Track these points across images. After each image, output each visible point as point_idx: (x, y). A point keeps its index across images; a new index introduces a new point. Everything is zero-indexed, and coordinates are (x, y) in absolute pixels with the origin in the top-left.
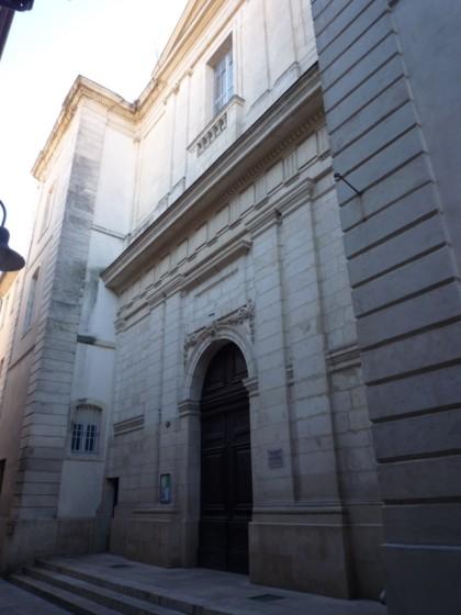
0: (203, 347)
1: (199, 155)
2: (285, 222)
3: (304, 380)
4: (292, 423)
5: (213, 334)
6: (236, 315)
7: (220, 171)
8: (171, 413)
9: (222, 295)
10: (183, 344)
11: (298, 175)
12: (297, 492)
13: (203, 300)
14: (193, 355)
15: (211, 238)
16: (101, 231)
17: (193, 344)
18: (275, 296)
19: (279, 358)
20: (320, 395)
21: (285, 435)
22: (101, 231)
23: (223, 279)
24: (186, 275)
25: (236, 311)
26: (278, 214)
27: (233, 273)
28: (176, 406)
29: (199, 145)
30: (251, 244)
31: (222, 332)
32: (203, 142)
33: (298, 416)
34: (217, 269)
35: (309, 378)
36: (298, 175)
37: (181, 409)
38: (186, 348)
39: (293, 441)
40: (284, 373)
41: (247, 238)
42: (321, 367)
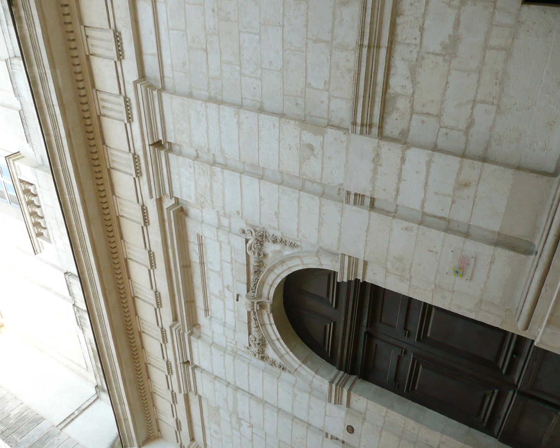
0: (273, 331)
1: (49, 240)
2: (171, 138)
3: (373, 180)
4: (424, 220)
5: (262, 306)
7: (73, 202)
10: (262, 363)
11: (125, 98)
12: (520, 247)
13: (216, 305)
14: (276, 350)
15: (140, 219)
16: (70, 419)
17: (262, 344)
18: (252, 185)
19: (332, 209)
20: (403, 160)
21: (435, 236)
22: (70, 419)
23: (202, 264)
24: (175, 319)
25: (248, 256)
26: (158, 144)
27: (201, 245)
28: (332, 408)
29: (39, 235)
30: (177, 199)
31: (265, 291)
32: (38, 227)
33: (418, 207)
34: (186, 266)
35: (375, 171)
36: (125, 98)
37: (338, 402)
39: (448, 226)
40: (355, 208)
41: (168, 203)
42: (366, 144)
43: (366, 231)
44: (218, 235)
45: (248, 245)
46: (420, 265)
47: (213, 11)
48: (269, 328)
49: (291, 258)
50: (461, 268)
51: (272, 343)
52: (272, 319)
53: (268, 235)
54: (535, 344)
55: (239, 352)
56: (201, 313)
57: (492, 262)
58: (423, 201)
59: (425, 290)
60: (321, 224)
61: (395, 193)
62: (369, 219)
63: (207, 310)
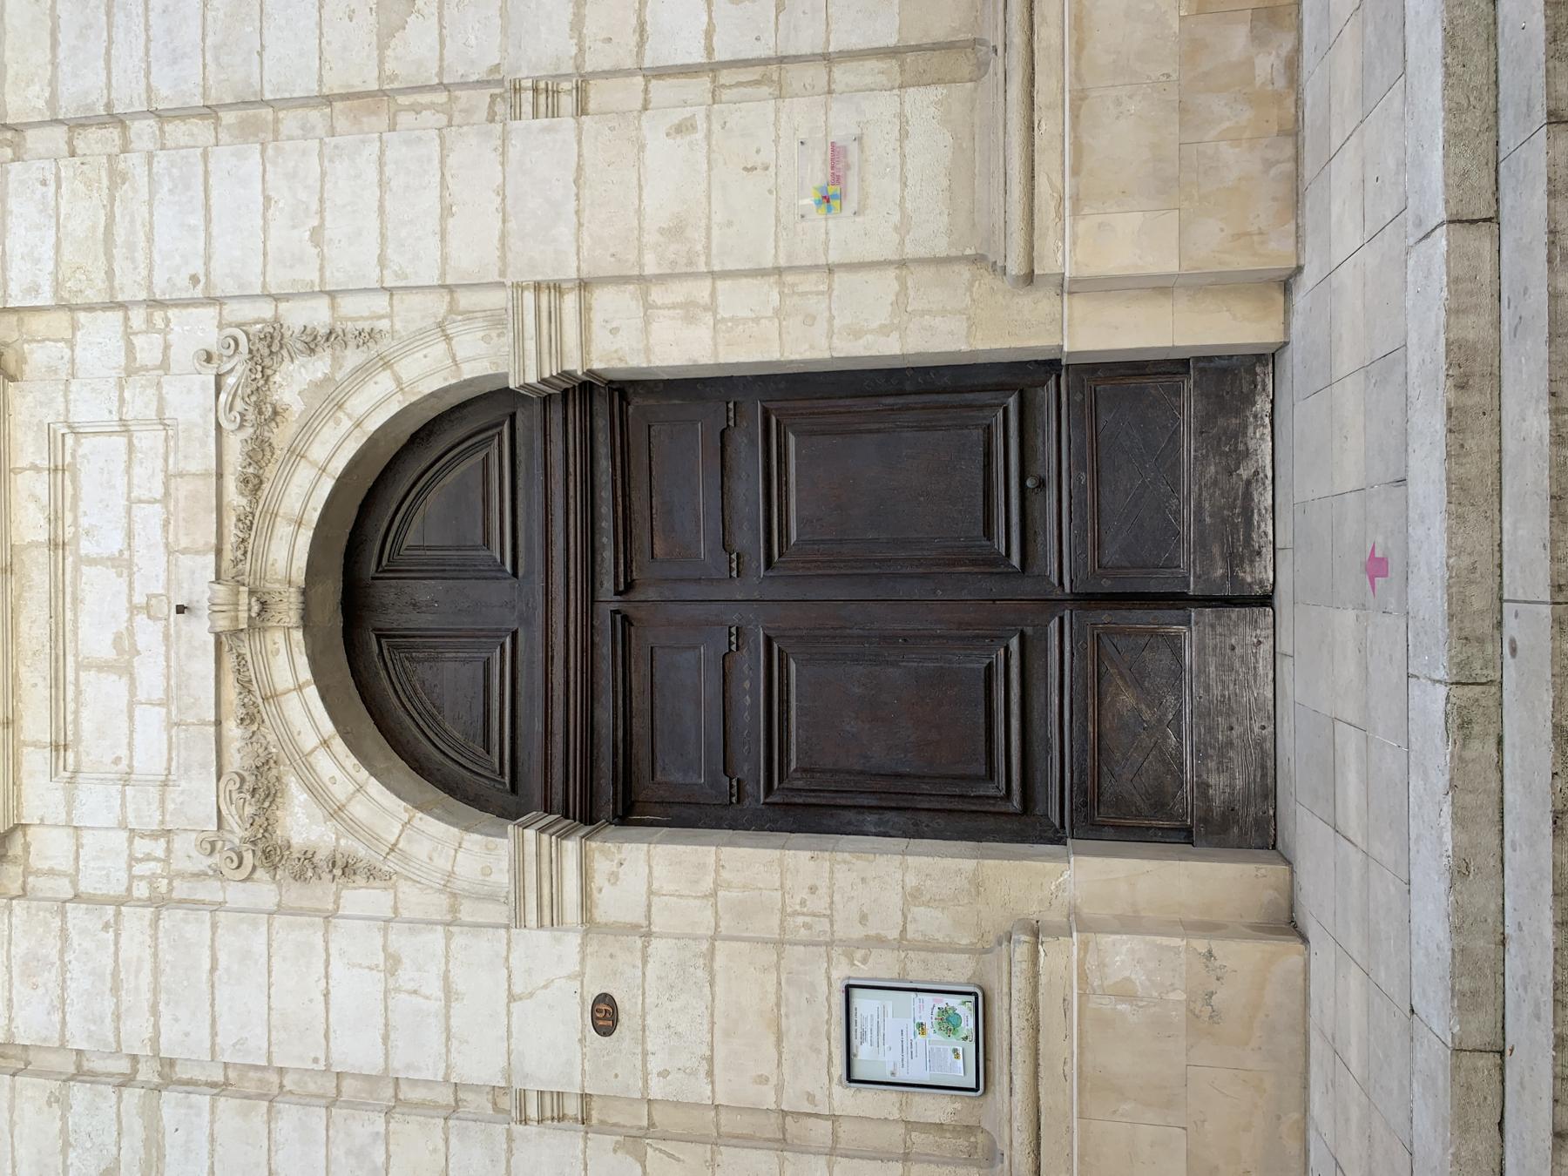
0: (305, 715)
8: (557, 967)
9: (123, 563)
10: (264, 891)
13: (99, 698)
14: (316, 791)
21: (753, 117)
28: (535, 942)
37: (551, 918)
38: (269, 852)
43: (576, 182)
44: (122, 400)
45: (223, 397)
46: (730, 224)
49: (364, 372)
50: (836, 179)
51: (304, 764)
52: (302, 661)
53: (287, 334)
54: (1066, 349)
55: (182, 890)
56: (35, 761)
57: (904, 135)
58: (709, 34)
59: (757, 320)
60: (446, 211)
61: (636, 37)
62: (579, 142)
63: (58, 747)
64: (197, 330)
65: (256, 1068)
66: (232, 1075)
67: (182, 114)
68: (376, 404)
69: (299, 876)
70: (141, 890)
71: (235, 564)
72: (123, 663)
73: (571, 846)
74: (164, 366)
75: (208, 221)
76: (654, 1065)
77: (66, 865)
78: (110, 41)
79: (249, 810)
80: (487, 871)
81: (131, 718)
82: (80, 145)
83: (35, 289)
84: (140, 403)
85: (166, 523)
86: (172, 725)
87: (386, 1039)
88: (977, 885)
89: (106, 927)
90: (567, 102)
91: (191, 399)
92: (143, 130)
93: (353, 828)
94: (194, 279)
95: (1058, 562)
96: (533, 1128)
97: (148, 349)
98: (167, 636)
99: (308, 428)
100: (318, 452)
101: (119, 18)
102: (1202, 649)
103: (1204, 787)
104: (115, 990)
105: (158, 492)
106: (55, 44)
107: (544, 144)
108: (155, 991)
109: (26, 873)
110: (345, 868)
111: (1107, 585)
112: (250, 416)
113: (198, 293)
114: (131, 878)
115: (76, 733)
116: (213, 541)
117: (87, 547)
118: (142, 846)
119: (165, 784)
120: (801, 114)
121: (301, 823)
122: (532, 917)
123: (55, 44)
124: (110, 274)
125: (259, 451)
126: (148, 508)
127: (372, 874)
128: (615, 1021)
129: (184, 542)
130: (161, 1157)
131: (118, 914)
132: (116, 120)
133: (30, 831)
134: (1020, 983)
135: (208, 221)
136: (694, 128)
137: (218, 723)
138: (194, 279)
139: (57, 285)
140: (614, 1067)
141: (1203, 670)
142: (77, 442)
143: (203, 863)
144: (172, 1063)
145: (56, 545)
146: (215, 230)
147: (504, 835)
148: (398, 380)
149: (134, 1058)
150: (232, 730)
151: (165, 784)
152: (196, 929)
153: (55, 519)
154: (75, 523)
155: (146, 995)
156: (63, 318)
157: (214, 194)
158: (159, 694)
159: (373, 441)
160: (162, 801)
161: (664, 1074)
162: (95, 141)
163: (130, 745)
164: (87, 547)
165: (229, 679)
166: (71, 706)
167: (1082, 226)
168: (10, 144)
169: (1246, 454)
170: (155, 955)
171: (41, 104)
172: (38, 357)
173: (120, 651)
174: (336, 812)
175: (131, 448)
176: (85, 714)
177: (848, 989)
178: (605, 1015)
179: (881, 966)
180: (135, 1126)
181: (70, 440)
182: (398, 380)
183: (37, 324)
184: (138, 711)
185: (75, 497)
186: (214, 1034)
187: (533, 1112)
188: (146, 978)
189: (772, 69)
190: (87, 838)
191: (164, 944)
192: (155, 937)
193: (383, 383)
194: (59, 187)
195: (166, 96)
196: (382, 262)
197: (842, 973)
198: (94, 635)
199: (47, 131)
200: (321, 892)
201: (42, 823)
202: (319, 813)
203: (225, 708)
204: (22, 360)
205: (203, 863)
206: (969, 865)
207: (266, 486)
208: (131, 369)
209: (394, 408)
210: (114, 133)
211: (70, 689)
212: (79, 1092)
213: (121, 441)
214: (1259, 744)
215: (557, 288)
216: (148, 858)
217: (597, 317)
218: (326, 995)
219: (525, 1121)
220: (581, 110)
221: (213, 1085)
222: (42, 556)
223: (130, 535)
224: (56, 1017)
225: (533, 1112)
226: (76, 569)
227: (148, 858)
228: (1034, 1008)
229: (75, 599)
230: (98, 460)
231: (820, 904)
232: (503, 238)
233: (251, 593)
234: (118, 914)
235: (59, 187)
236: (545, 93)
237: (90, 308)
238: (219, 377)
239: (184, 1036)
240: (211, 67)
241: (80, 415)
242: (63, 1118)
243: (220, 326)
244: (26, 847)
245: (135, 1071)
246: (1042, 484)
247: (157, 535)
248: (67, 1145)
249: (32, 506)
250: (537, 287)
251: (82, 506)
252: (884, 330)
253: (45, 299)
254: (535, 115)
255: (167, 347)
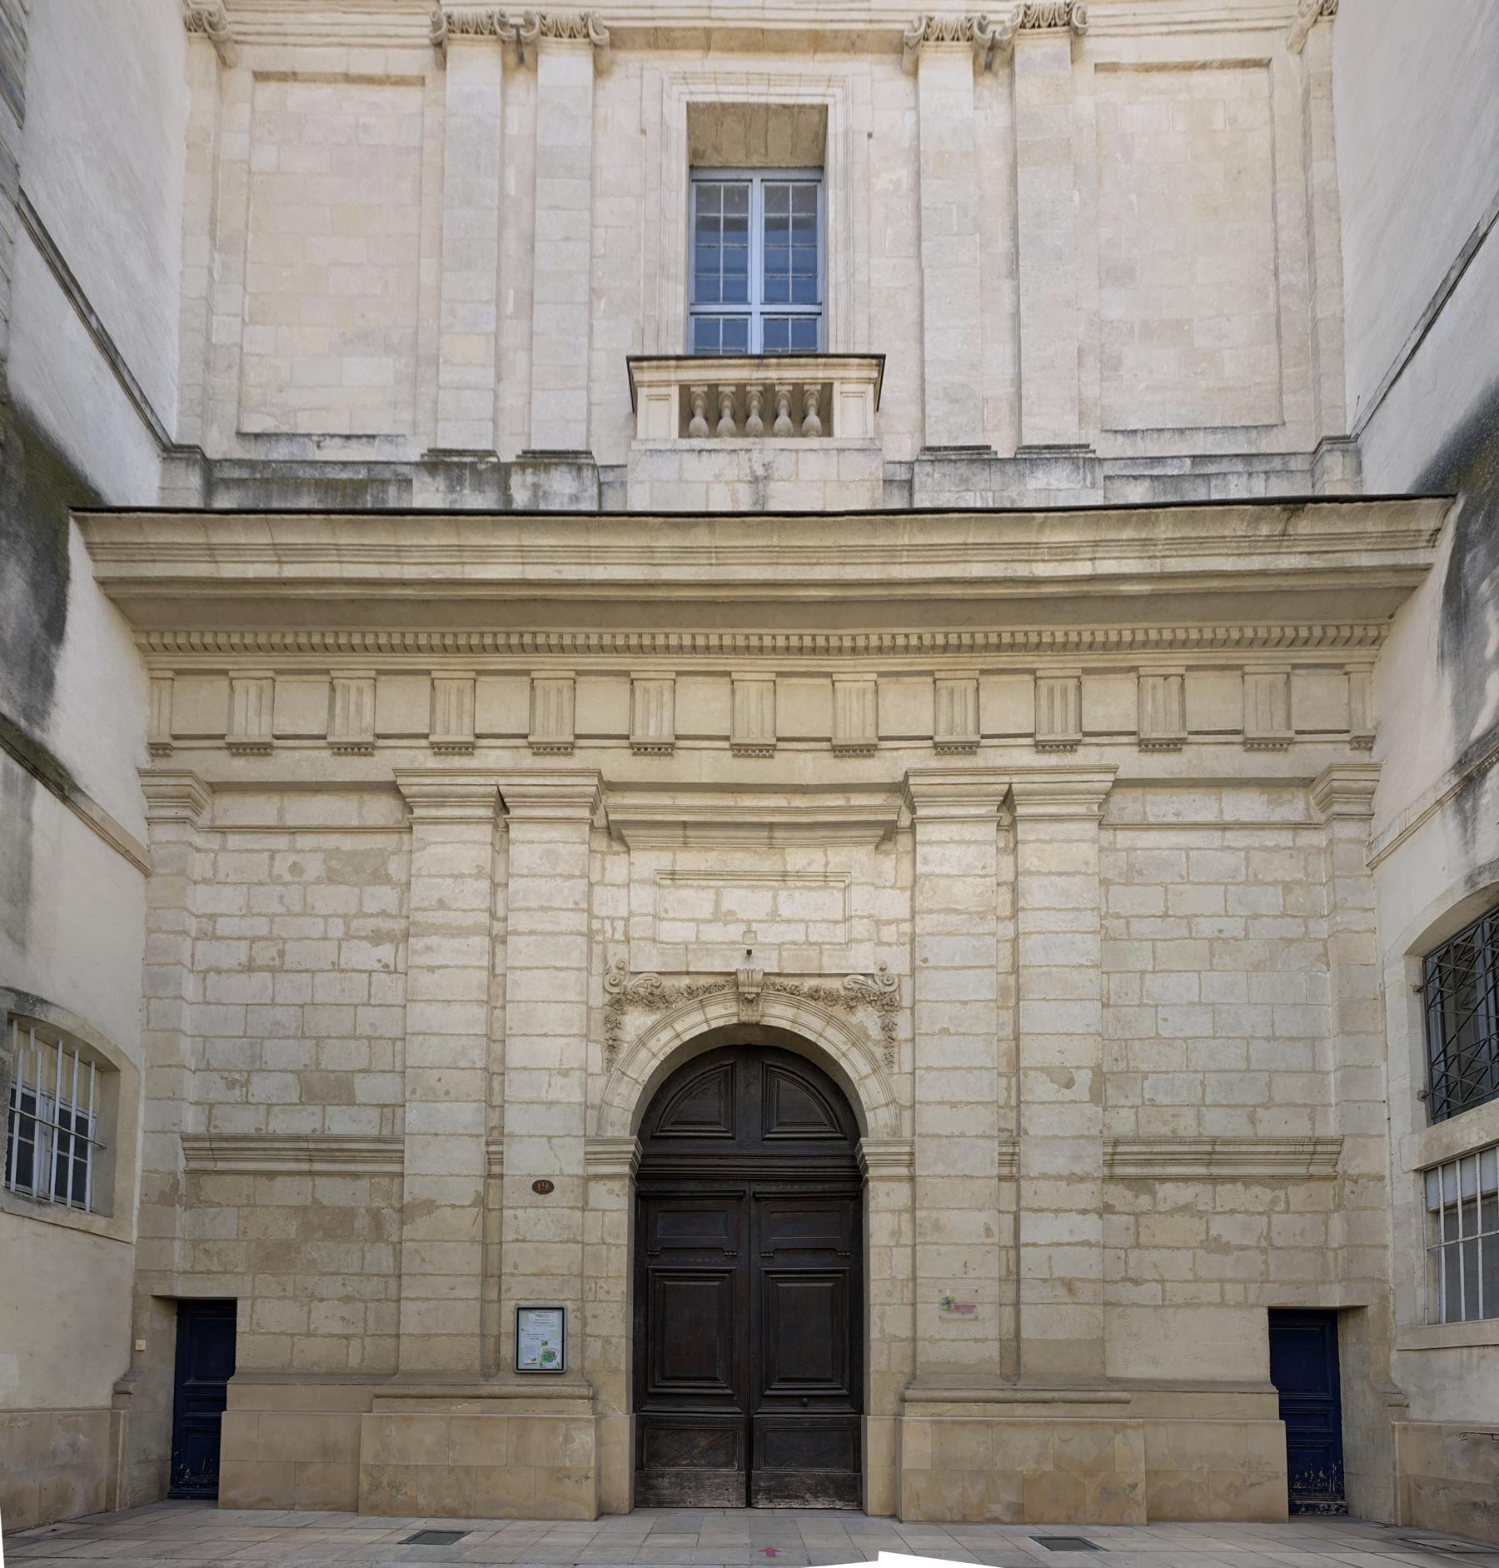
0: (693, 1024)
6: (834, 985)
8: (566, 1162)
9: (774, 917)
10: (599, 999)
13: (699, 901)
14: (652, 1031)
17: (654, 999)
38: (619, 1002)
44: (862, 917)
47: (1220, 931)
48: (697, 1017)
49: (871, 1058)
51: (667, 1023)
52: (721, 1023)
55: (597, 949)
56: (664, 860)
63: (673, 875)
64: (898, 963)
65: (504, 993)
66: (500, 979)
67: (1015, 953)
68: (854, 1065)
69: (607, 1020)
70: (596, 925)
71: (774, 985)
72: (721, 917)
73: (626, 1169)
74: (880, 943)
75: (956, 968)
76: (520, 1212)
77: (609, 877)
78: (1059, 910)
79: (641, 990)
80: (613, 1124)
81: (689, 920)
82: (1003, 889)
83: (926, 862)
84: (860, 928)
85: (795, 943)
86: (686, 944)
87: (525, 1068)
88: (615, 1371)
89: (576, 903)
90: (1006, 1171)
91: (862, 959)
92: (1008, 930)
93: (634, 1052)
94: (925, 960)
95: (766, 1413)
96: (483, 1148)
97: (889, 933)
98: (734, 943)
99: (843, 1027)
100: (830, 1032)
101: (1071, 916)
102: (727, 1476)
103: (663, 1476)
104: (542, 909)
105: (812, 939)
106: (1060, 874)
107: (984, 1159)
108: (542, 933)
109: (603, 853)
110: (612, 1047)
111: (757, 1434)
112: (851, 994)
113: (918, 963)
114: (603, 919)
115: (681, 886)
116: (786, 971)
117: (783, 894)
118: (620, 925)
119: (654, 940)
120: (991, 1290)
121: (636, 1021)
122: (590, 1149)
123: (1060, 874)
124: (930, 912)
125: (831, 998)
126: (803, 932)
127: (610, 1061)
128: (541, 1192)
129: (785, 954)
130: (453, 936)
131: (583, 911)
132: (1016, 911)
133: (625, 856)
134: (569, 1390)
135: (956, 968)
136: (988, 1236)
137: (688, 973)
138: (925, 960)
139: (927, 876)
140: (517, 1192)
141: (717, 1476)
142: (839, 890)
143: (612, 963)
144: (504, 942)
145: (784, 876)
146: (952, 972)
147: (632, 1134)
148: (866, 1077)
149: (505, 919)
150: (685, 981)
151: (654, 940)
152: (577, 959)
153: (799, 875)
154: (796, 888)
155: (540, 928)
156: (908, 882)
157: (970, 972)
158: (703, 938)
159: (835, 1063)
160: (644, 939)
161: (516, 1217)
162: (1005, 895)
163: (674, 919)
164: (783, 894)
165: (711, 980)
166: (695, 883)
167: (927, 1425)
168: (1006, 846)
169: (816, 1497)
170: (562, 933)
171: (1027, 865)
172: (888, 864)
173: (725, 914)
174: (642, 1042)
175: (836, 922)
176: (690, 892)
177: (562, 1309)
178: (543, 1187)
179: (573, 1325)
180: (470, 920)
181: (842, 885)
182: (866, 1077)
183: (906, 863)
184: (693, 924)
185: (810, 888)
186: (521, 969)
187: (492, 1148)
188: (550, 928)
189: (1014, 1276)
190: (623, 892)
191: (569, 938)
192: (571, 933)
193: (865, 1068)
194: (981, 876)
195: (1026, 944)
196: (929, 1068)
197: (569, 1306)
198: (736, 899)
199: (1012, 868)
200: (599, 1032)
201: (631, 864)
202: (641, 1032)
203: (695, 977)
204: (887, 853)
205: (612, 963)
206: (623, 1367)
207: (813, 1003)
208: (878, 923)
209: (852, 1075)
210: (1008, 913)
211: (704, 883)
212: (484, 885)
213: (839, 917)
214: (683, 1501)
215: (911, 1164)
216: (614, 929)
217: (895, 1185)
218: (545, 1035)
219: (488, 1144)
220: (1001, 1178)
221: (493, 968)
222: (778, 867)
223: (789, 921)
224: (525, 872)
225: (492, 1148)
226: (771, 888)
227: (614, 929)
228: (559, 1397)
229: (754, 887)
230: (828, 902)
231: (601, 1296)
232: (939, 1136)
233: (758, 994)
234: (583, 911)
235: (981, 876)
236: (1011, 1159)
237: (912, 899)
238: (872, 975)
239: (520, 950)
240: (1040, 970)
241: (856, 892)
242: (471, 875)
243: (899, 975)
244: (617, 853)
245: (498, 920)
246: (804, 1405)
247: (789, 938)
248: (456, 877)
249: (805, 861)
250: (912, 1154)
251: (805, 892)
252: (882, 1331)
253: (920, 868)
254: (1000, 1154)
255: (889, 945)
